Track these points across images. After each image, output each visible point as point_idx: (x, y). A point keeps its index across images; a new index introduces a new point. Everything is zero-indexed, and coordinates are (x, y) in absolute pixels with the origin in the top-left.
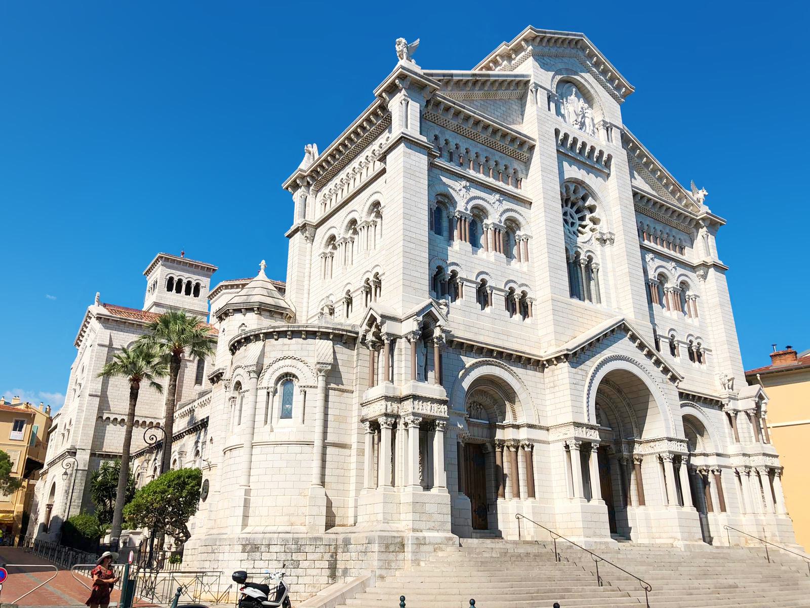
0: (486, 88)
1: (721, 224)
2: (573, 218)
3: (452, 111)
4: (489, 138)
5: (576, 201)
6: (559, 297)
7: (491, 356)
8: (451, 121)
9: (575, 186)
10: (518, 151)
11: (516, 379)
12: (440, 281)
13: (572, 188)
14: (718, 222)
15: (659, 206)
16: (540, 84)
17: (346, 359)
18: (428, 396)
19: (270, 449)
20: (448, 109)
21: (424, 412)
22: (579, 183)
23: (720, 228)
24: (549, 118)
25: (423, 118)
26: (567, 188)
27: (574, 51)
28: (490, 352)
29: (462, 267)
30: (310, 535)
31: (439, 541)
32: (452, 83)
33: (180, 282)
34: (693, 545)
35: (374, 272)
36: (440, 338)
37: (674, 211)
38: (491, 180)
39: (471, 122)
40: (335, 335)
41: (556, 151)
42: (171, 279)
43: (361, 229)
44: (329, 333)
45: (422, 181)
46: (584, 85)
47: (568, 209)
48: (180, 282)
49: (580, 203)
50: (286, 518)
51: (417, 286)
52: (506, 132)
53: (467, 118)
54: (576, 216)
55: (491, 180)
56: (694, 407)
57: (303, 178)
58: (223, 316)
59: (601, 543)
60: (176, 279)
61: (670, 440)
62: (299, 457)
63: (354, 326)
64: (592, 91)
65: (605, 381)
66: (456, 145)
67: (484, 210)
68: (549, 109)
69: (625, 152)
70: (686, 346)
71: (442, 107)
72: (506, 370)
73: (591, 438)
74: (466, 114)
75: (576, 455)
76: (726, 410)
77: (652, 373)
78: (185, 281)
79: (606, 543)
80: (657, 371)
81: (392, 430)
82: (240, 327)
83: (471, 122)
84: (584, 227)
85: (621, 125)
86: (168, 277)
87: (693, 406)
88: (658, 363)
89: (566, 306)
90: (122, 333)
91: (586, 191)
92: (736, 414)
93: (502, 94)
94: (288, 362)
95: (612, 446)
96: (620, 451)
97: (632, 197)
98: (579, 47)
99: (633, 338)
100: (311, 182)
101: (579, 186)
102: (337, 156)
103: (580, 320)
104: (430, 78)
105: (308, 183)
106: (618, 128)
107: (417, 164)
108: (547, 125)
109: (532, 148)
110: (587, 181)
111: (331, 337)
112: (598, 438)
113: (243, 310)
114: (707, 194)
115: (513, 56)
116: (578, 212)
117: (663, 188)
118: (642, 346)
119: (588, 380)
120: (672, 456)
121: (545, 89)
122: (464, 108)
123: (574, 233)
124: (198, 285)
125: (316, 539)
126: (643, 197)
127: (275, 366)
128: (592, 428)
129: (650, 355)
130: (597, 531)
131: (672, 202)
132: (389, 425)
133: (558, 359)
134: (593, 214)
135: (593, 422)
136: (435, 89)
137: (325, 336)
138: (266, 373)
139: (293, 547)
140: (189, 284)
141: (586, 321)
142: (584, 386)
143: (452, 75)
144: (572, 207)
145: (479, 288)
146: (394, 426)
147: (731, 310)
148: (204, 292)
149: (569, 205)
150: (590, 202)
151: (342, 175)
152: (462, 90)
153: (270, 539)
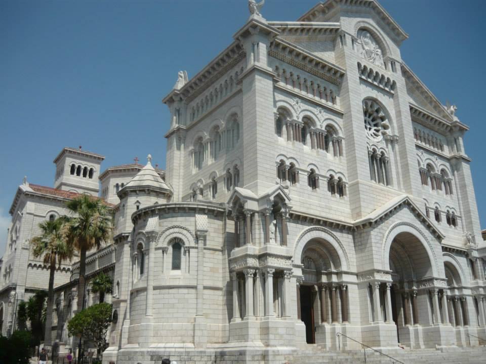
0: (310, 34)
1: (466, 130)
2: (370, 125)
3: (288, 50)
5: (372, 113)
7: (320, 225)
9: (372, 103)
10: (333, 77)
11: (336, 240)
12: (282, 171)
13: (369, 103)
14: (464, 128)
15: (438, 123)
16: (346, 31)
17: (217, 227)
18: (278, 254)
19: (167, 291)
20: (284, 48)
21: (276, 265)
22: (374, 101)
23: (466, 133)
25: (269, 54)
26: (366, 104)
27: (368, 9)
28: (318, 222)
29: (298, 160)
30: (196, 350)
31: (288, 353)
32: (287, 30)
33: (79, 167)
34: (449, 348)
35: (234, 164)
36: (286, 213)
37: (436, 120)
38: (317, 99)
39: (301, 57)
40: (210, 211)
41: (358, 78)
42: (73, 167)
43: (222, 133)
44: (204, 209)
45: (269, 99)
46: (375, 33)
48: (79, 167)
49: (375, 114)
50: (180, 338)
51: (268, 175)
52: (324, 64)
53: (298, 55)
54: (372, 123)
55: (317, 99)
57: (176, 95)
58: (123, 195)
59: (392, 350)
60: (77, 166)
61: (437, 279)
62: (187, 296)
63: (221, 204)
64: (381, 37)
65: (395, 240)
66: (291, 73)
67: (312, 120)
68: (353, 49)
69: (403, 79)
70: (445, 214)
71: (281, 47)
72: (329, 234)
73: (387, 280)
74: (298, 52)
75: (377, 293)
76: (470, 257)
77: (426, 234)
78: (83, 167)
79: (396, 350)
80: (427, 233)
81: (253, 278)
82: (136, 203)
83: (301, 57)
84: (378, 131)
85: (400, 61)
86: (71, 164)
87: (449, 256)
88: (429, 227)
90: (42, 205)
92: (476, 260)
93: (321, 37)
94: (176, 230)
95: (397, 284)
96: (402, 287)
97: (409, 111)
98: (371, 6)
99: (413, 210)
100: (183, 98)
101: (374, 103)
102: (203, 80)
103: (379, 198)
104: (272, 26)
105: (181, 99)
106: (399, 62)
107: (266, 87)
109: (342, 75)
110: (379, 99)
111: (206, 212)
112: (391, 280)
113: (137, 192)
114: (456, 108)
115: (327, 12)
116: (373, 120)
118: (418, 216)
119: (384, 240)
120: (437, 290)
121: (350, 35)
122: (296, 47)
123: (371, 135)
124: (91, 171)
125: (201, 352)
126: (416, 110)
127: (167, 233)
128: (387, 273)
129: (423, 221)
131: (435, 115)
132: (251, 274)
133: (364, 225)
134: (384, 122)
135: (388, 268)
136: (276, 35)
137: (202, 211)
138: (161, 238)
139: (186, 357)
140: (85, 169)
141: (382, 198)
142: (382, 244)
143: (287, 25)
144: (369, 117)
145: (309, 175)
146: (255, 275)
147: (473, 189)
148: (96, 175)
149: (368, 116)
150: (381, 114)
151: (207, 93)
152: (294, 35)
153: (170, 352)
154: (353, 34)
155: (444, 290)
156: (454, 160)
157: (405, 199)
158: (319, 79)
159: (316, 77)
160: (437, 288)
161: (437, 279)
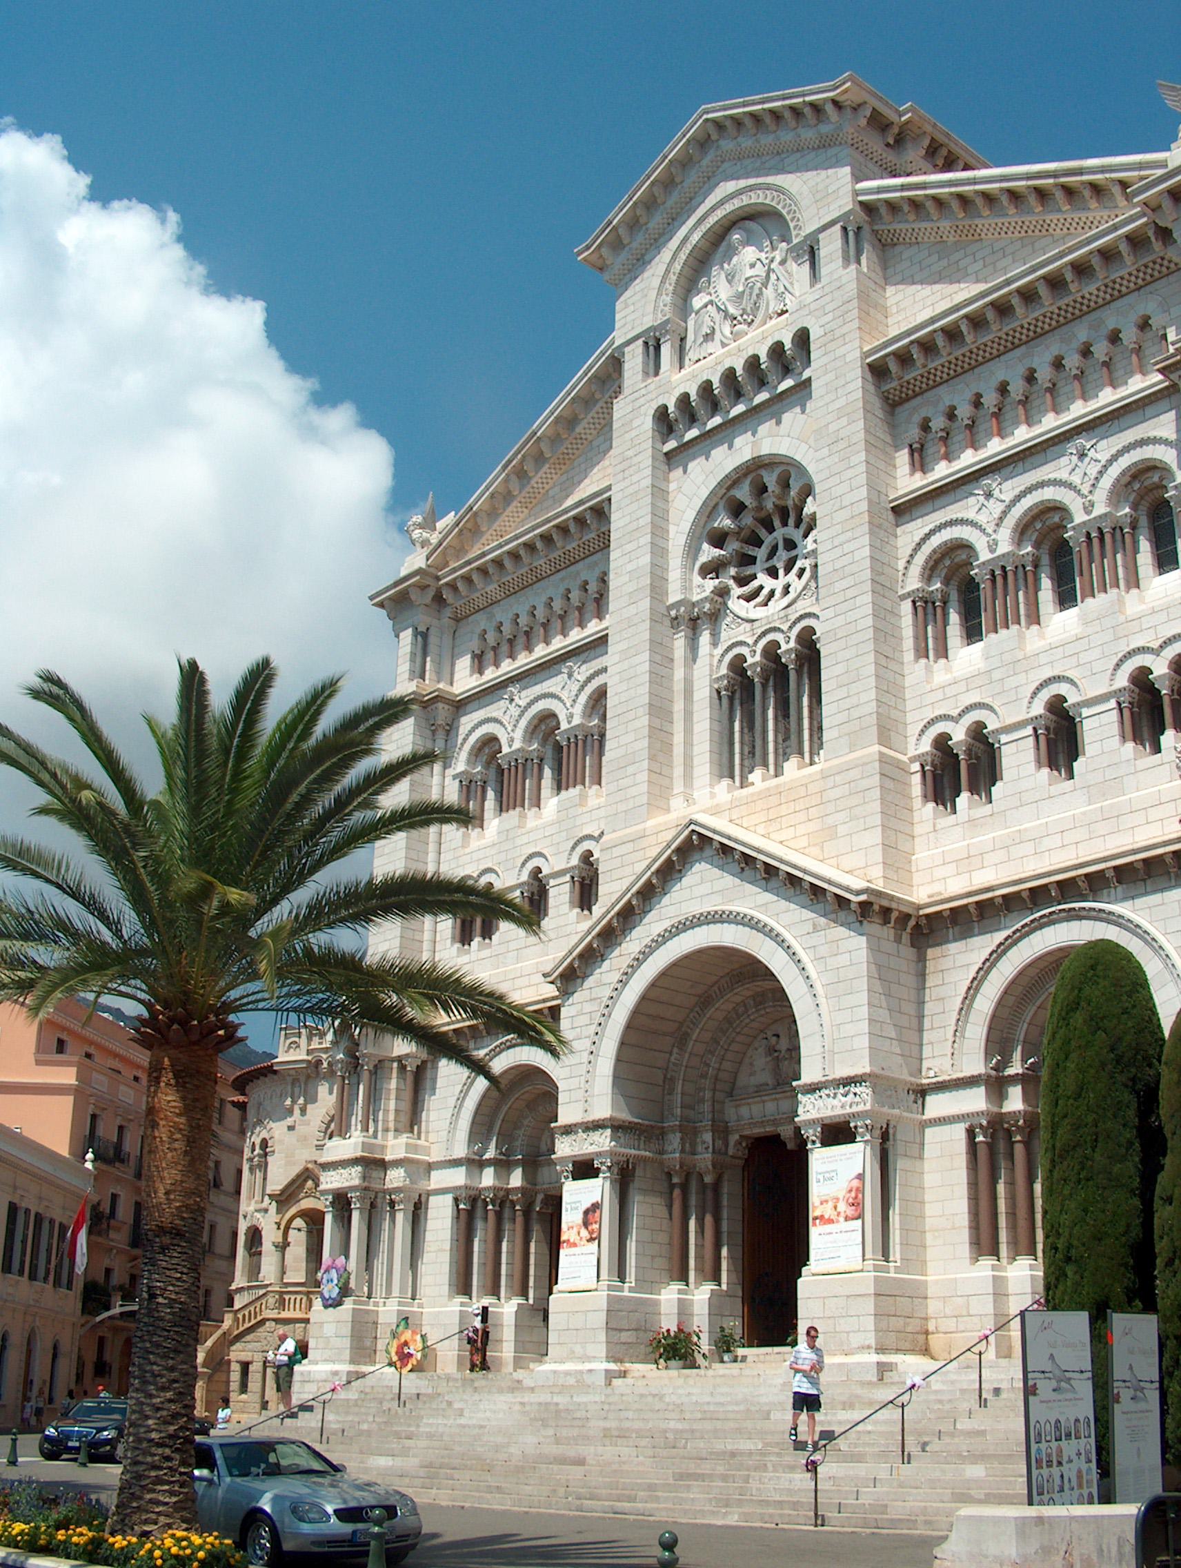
4: (551, 557)
6: (628, 831)
8: (488, 589)
13: (743, 493)
22: (754, 469)
24: (642, 401)
31: (324, 1377)
39: (508, 563)
47: (780, 533)
56: (1080, 918)
59: (567, 1373)
61: (813, 1089)
89: (630, 847)
91: (782, 468)
101: (763, 473)
108: (635, 424)
117: (1048, 218)
128: (596, 1126)
130: (578, 1349)
144: (785, 524)
154: (648, 322)
155: (852, 1125)
156: (1174, 377)
157: (686, 832)
158: (580, 565)
159: (572, 569)
160: (813, 1122)
161: (813, 1089)
